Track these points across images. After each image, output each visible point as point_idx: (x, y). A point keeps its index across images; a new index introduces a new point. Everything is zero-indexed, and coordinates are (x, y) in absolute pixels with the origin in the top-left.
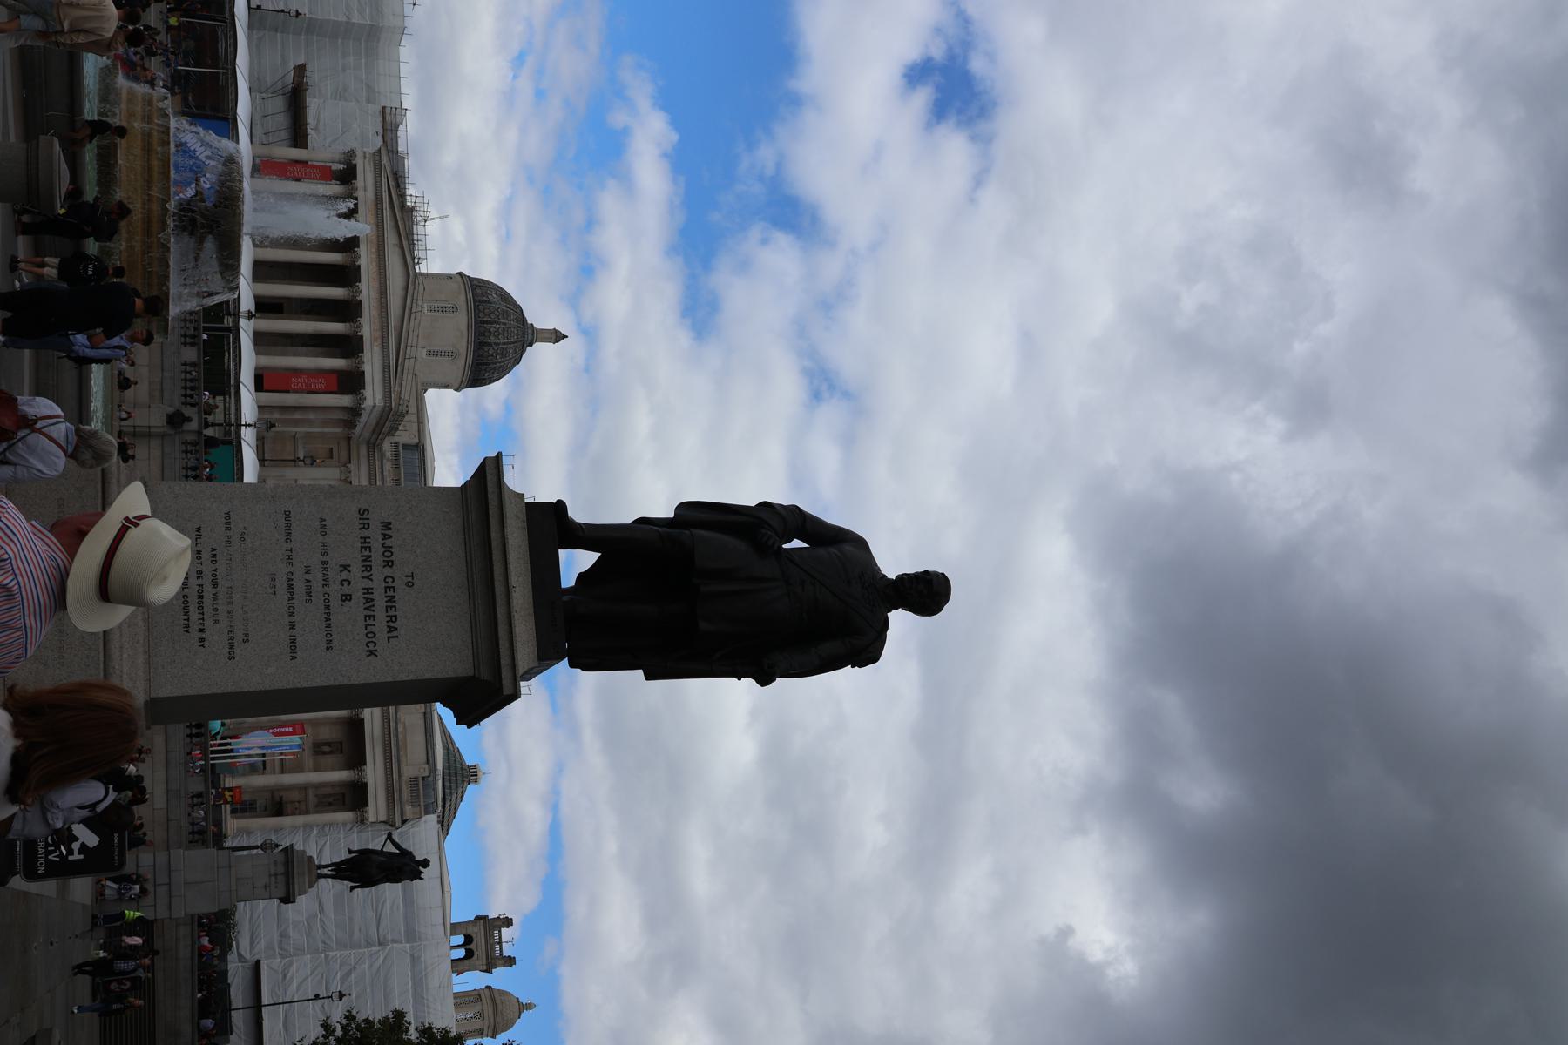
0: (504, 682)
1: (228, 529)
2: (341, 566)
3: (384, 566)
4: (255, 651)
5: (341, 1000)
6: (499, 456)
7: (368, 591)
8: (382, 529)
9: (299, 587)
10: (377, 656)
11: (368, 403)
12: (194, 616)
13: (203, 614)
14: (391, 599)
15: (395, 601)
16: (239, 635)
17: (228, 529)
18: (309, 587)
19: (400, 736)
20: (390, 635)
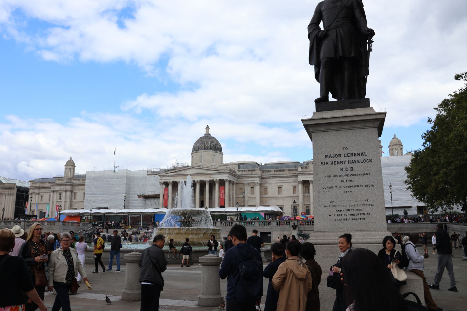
0: (381, 117)
1: (329, 206)
2: (341, 171)
3: (341, 157)
4: (371, 198)
6: (303, 121)
7: (349, 162)
8: (328, 158)
9: (349, 184)
10: (372, 159)
11: (228, 178)
12: (359, 216)
13: (358, 214)
14: (352, 155)
15: (353, 153)
16: (366, 203)
17: (329, 206)
18: (349, 181)
20: (364, 155)
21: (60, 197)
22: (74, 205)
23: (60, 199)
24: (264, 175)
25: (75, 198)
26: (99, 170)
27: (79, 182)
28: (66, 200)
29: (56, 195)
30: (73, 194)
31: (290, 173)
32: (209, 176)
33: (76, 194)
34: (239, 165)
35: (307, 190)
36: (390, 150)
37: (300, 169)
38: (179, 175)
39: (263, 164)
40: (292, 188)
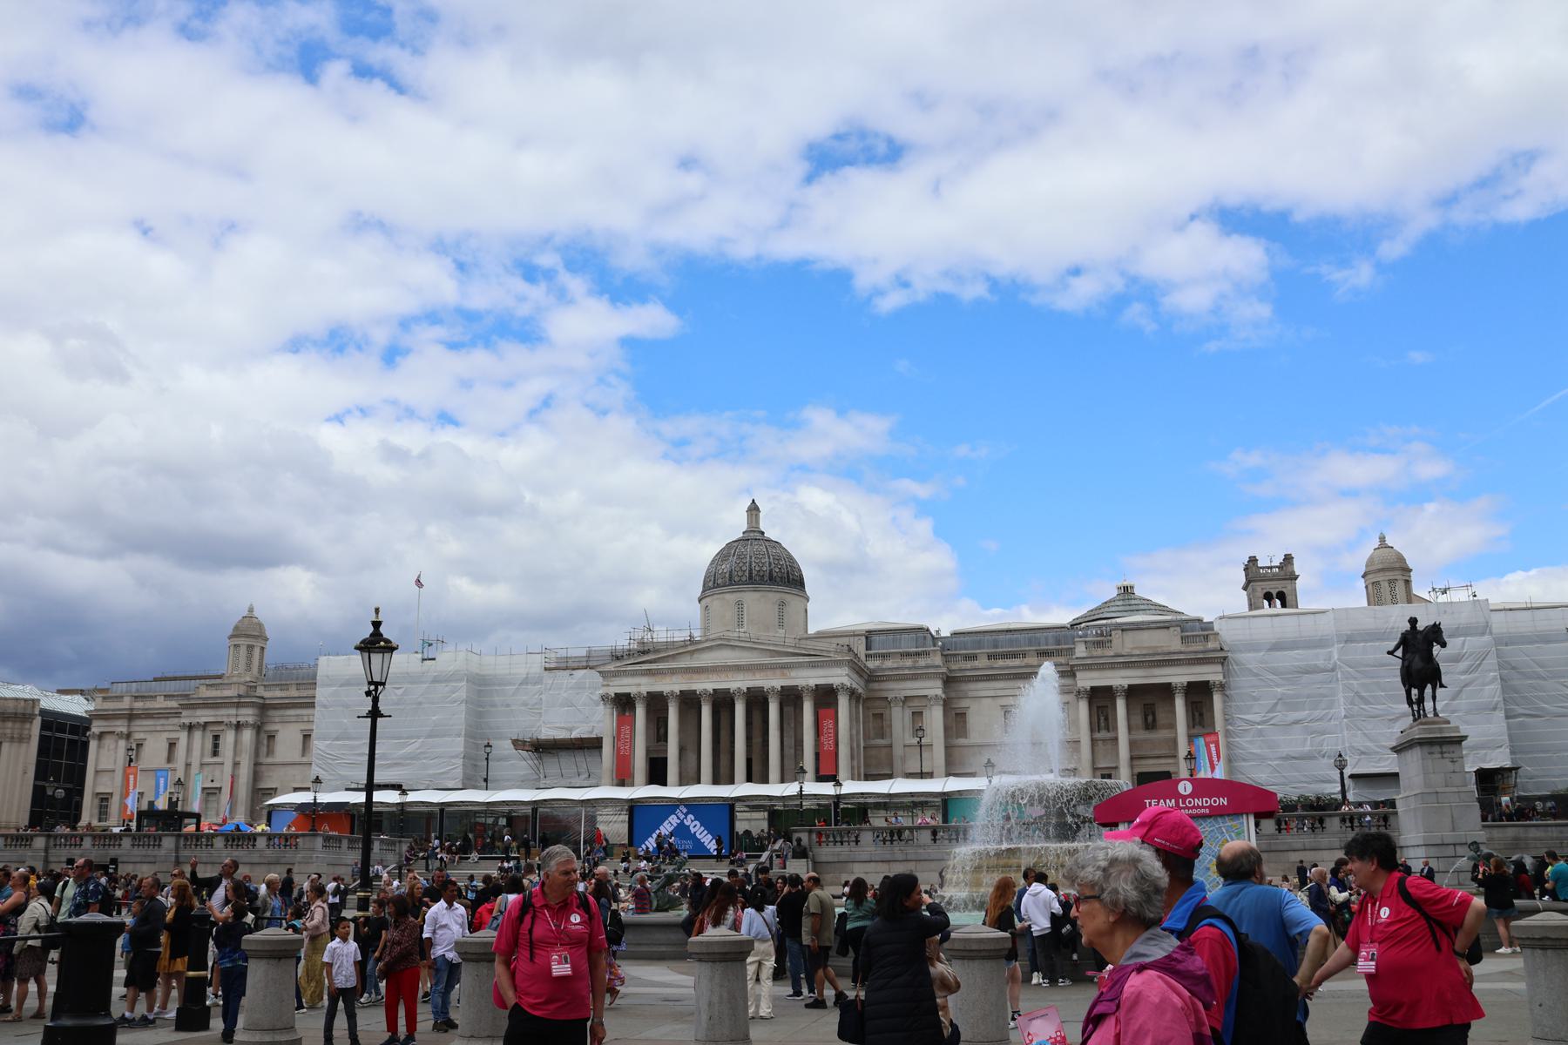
11: (847, 681)
19: (1144, 652)
21: (216, 746)
22: (266, 774)
23: (215, 753)
24: (954, 670)
25: (270, 752)
27: (283, 694)
28: (237, 759)
29: (200, 741)
30: (264, 737)
32: (778, 672)
34: (869, 635)
35: (1102, 718)
37: (1081, 651)
38: (673, 671)
39: (945, 633)
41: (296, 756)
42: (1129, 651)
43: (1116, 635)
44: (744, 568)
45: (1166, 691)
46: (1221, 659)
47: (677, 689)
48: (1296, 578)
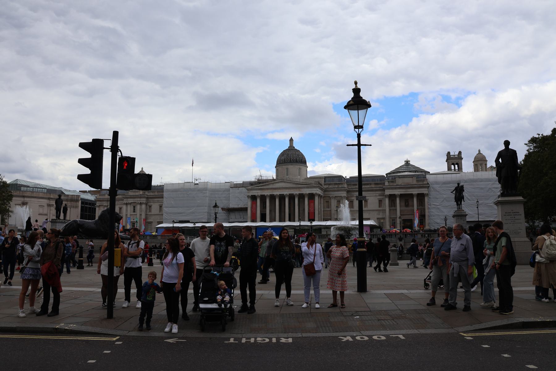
5: (479, 202)
9: (514, 222)
12: (517, 233)
16: (519, 229)
21: (134, 209)
23: (134, 212)
25: (150, 211)
26: (178, 183)
27: (153, 194)
28: (141, 213)
31: (376, 187)
32: (298, 189)
33: (151, 207)
35: (393, 203)
36: (475, 166)
37: (387, 184)
38: (268, 189)
39: (348, 177)
40: (377, 201)
41: (158, 212)
42: (400, 184)
43: (397, 179)
44: (288, 158)
45: (411, 196)
46: (427, 186)
47: (269, 194)
48: (462, 159)
